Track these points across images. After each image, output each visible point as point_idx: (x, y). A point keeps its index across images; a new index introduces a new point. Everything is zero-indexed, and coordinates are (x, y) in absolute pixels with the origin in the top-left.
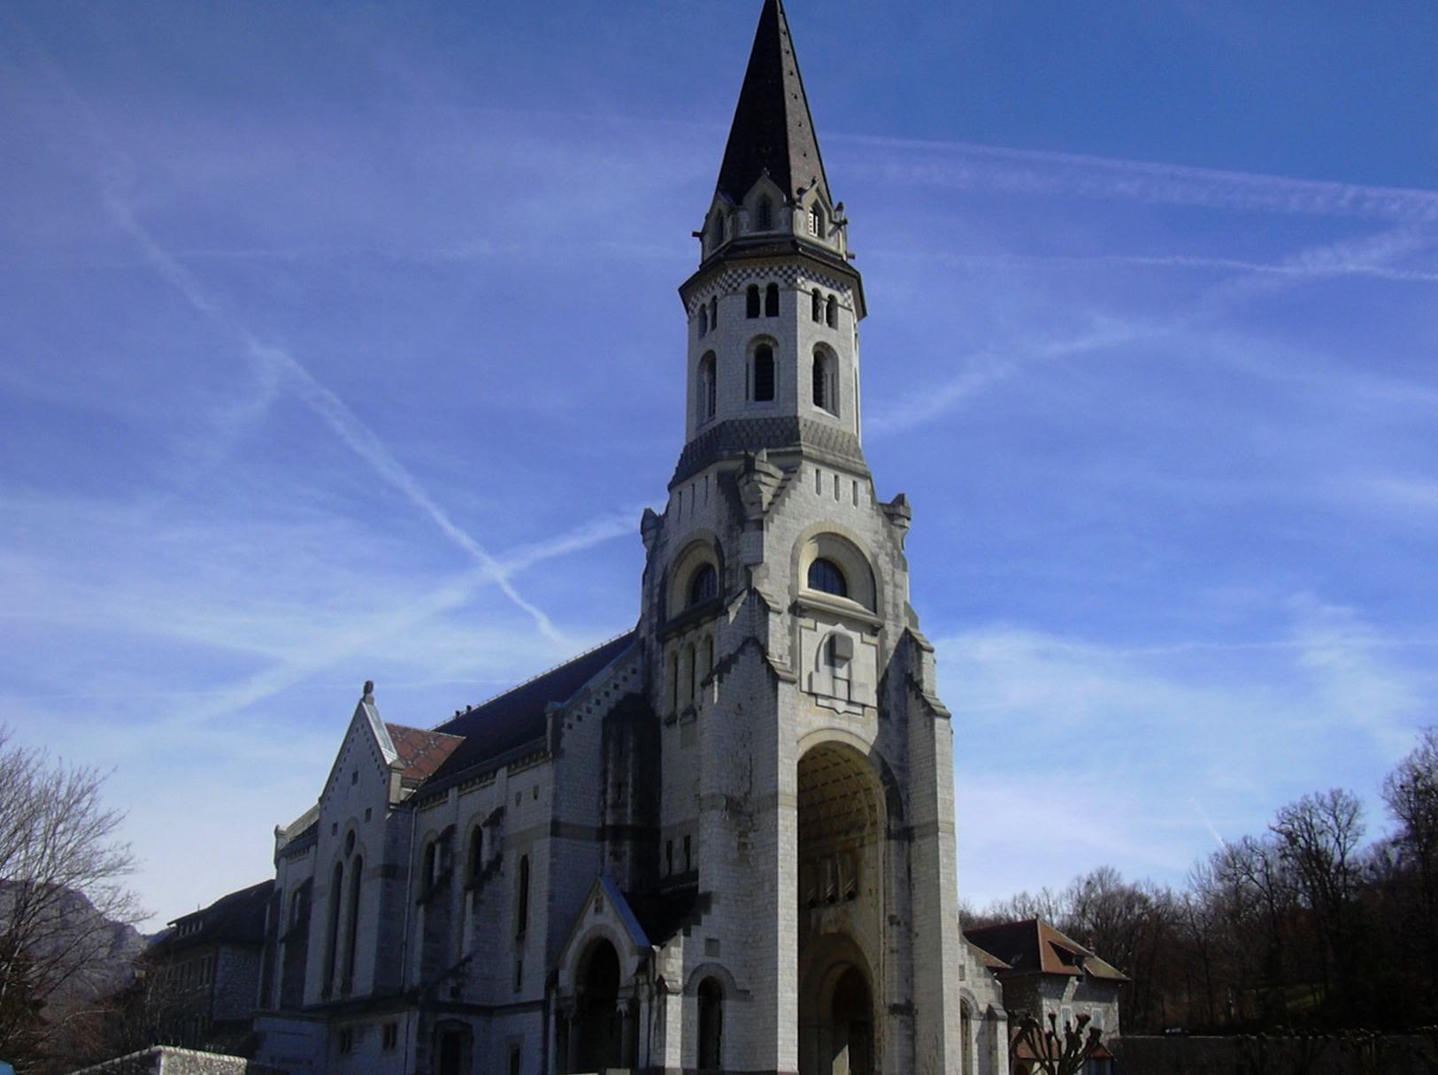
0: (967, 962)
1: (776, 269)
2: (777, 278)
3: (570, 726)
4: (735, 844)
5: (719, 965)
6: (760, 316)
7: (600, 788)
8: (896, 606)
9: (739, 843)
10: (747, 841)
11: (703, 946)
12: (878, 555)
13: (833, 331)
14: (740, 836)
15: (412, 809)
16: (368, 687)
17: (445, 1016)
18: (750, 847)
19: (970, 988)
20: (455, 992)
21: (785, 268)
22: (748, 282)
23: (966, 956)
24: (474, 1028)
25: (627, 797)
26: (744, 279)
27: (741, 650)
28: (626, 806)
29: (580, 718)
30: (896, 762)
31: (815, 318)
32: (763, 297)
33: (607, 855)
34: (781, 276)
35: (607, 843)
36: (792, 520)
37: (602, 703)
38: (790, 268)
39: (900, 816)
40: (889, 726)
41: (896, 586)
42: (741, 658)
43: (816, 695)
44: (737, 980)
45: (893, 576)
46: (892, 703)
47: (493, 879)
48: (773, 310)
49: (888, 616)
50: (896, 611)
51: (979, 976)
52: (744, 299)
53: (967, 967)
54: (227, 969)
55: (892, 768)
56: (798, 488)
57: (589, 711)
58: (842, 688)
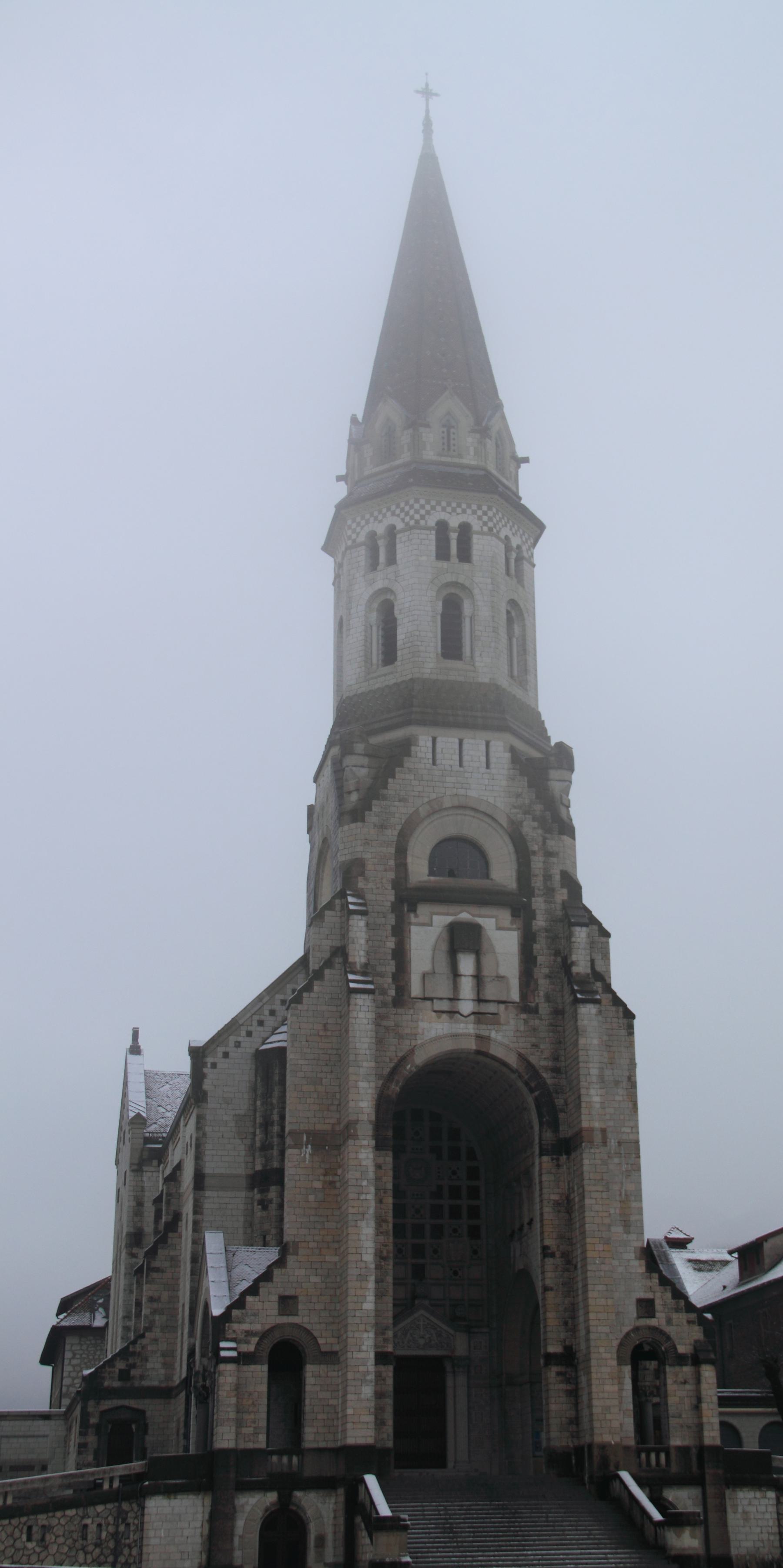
1: (393, 508)
2: (395, 518)
3: (214, 1065)
4: (318, 1185)
5: (296, 1324)
6: (379, 568)
7: (251, 1130)
8: (548, 877)
9: (325, 1182)
10: (337, 1178)
11: (276, 1305)
12: (521, 823)
13: (466, 566)
14: (325, 1175)
15: (159, 1166)
16: (136, 1034)
17: (107, 1404)
18: (338, 1185)
20: (124, 1375)
21: (402, 505)
22: (367, 529)
24: (148, 1414)
25: (272, 1137)
26: (362, 528)
27: (328, 964)
28: (272, 1149)
29: (226, 1055)
30: (549, 1063)
31: (442, 553)
32: (382, 544)
33: (256, 1204)
34: (398, 516)
35: (256, 1190)
36: (396, 803)
37: (254, 1034)
38: (407, 503)
39: (555, 1125)
40: (537, 1022)
41: (549, 854)
42: (327, 972)
43: (431, 999)
44: (321, 1341)
45: (544, 843)
46: (542, 994)
47: (169, 1241)
48: (392, 560)
49: (537, 892)
50: (549, 883)
52: (362, 551)
54: (74, 1362)
55: (540, 1071)
56: (406, 765)
57: (238, 1044)
58: (467, 987)
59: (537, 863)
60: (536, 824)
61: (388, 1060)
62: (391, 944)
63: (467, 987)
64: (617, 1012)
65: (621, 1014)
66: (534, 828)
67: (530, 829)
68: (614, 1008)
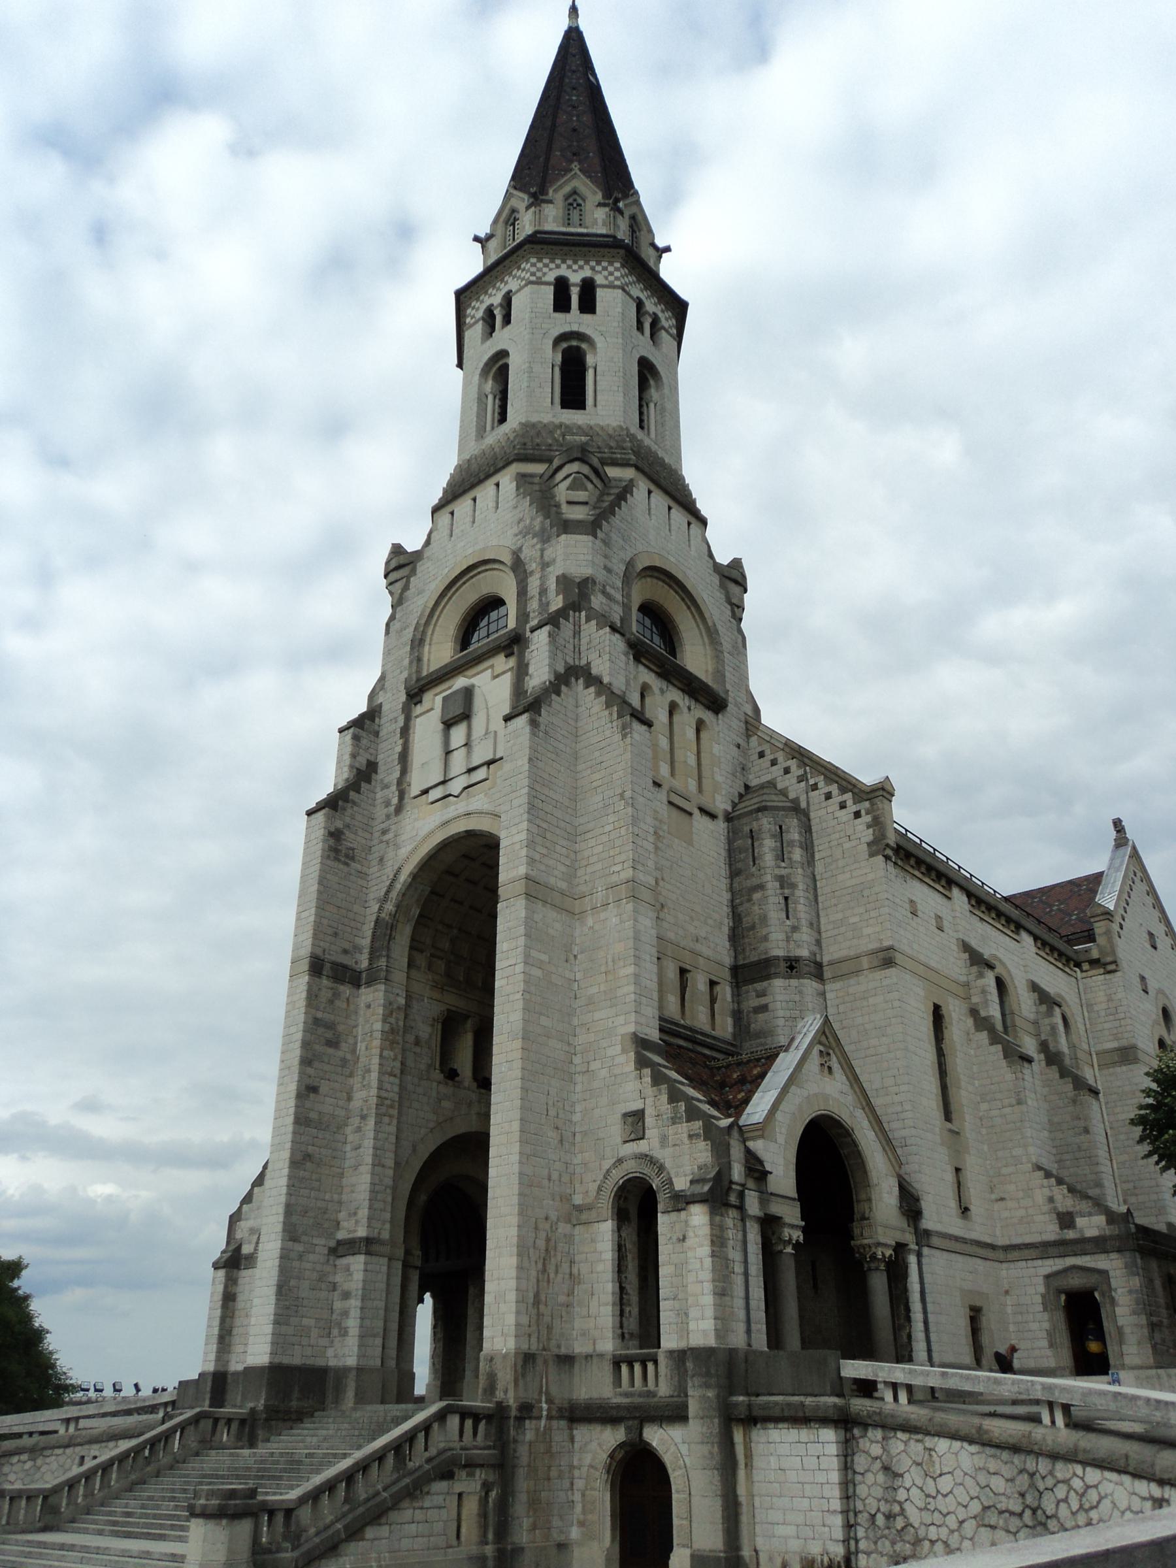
0: (649, 1101)
12: (520, 549)
19: (658, 1154)
23: (649, 1091)
45: (542, 556)
49: (532, 615)
51: (674, 1121)
53: (647, 1113)
59: (534, 584)
60: (535, 540)
61: (385, 878)
62: (399, 749)
63: (458, 762)
64: (611, 714)
65: (615, 716)
66: (533, 546)
67: (530, 552)
68: (607, 713)
